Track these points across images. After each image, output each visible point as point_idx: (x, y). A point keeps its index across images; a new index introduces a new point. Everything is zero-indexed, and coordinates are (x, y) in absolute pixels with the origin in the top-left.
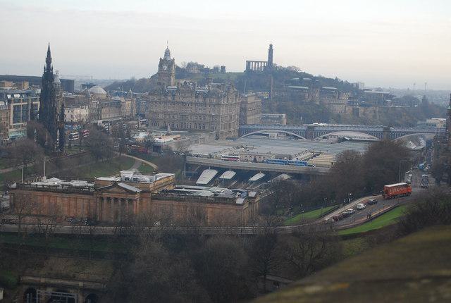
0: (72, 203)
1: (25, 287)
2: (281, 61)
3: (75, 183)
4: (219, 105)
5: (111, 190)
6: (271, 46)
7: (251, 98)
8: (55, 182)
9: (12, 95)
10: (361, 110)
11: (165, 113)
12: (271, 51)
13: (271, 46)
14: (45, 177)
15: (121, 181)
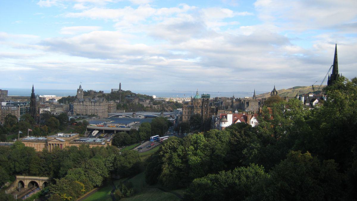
0: (39, 146)
1: (18, 181)
2: (124, 88)
3: (41, 138)
4: (100, 105)
5: (53, 141)
6: (120, 83)
7: (112, 103)
8: (33, 138)
9: (20, 104)
10: (154, 106)
11: (80, 109)
12: (120, 85)
13: (120, 83)
14: (28, 137)
15: (58, 137)
